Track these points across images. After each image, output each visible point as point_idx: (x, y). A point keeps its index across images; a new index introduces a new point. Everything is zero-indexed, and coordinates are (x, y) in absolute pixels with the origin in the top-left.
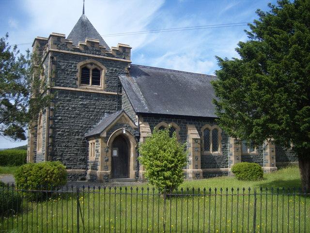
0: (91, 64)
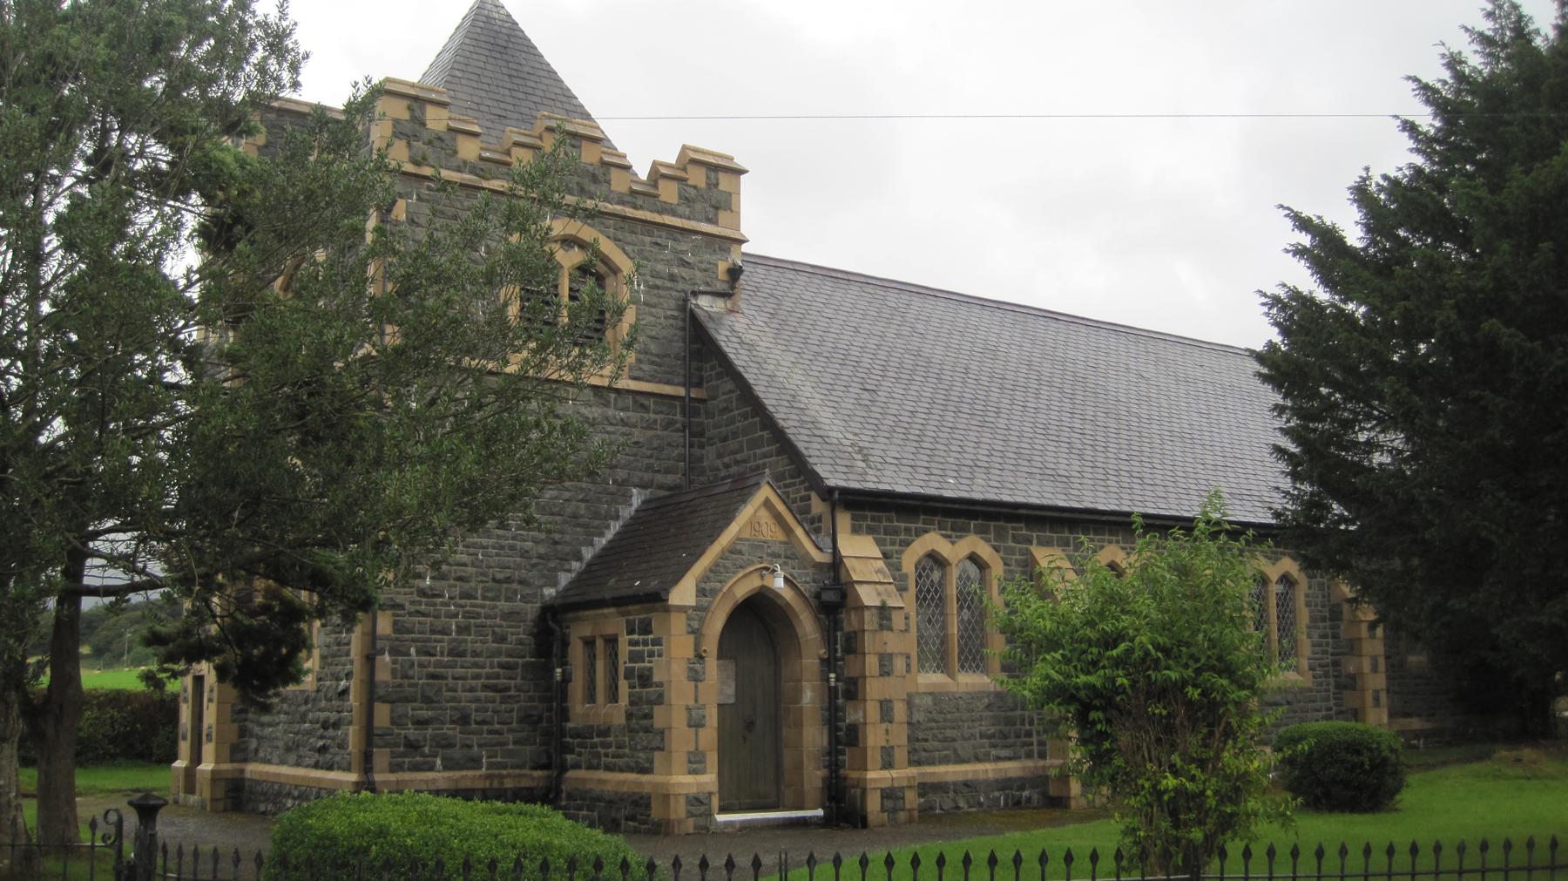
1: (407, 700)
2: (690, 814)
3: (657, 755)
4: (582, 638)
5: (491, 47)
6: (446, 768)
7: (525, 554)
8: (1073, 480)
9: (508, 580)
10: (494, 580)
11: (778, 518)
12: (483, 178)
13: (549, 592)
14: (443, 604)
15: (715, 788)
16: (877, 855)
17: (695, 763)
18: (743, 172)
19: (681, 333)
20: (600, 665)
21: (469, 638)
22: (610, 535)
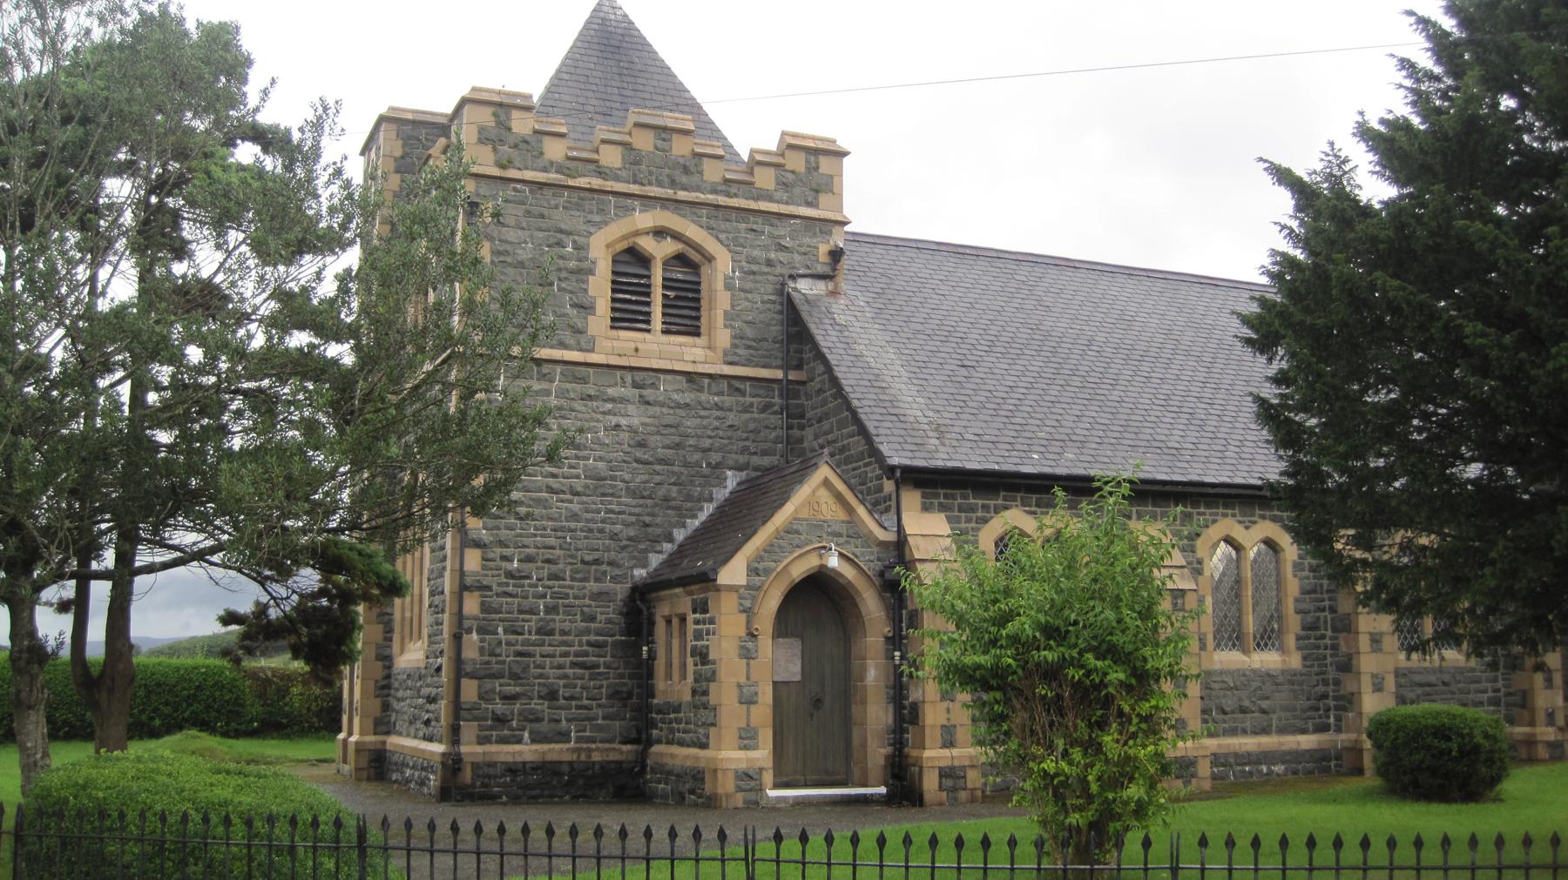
0: (660, 233)
1: (494, 676)
2: (739, 789)
3: (712, 730)
4: (663, 617)
5: (603, 48)
6: (533, 741)
7: (614, 537)
8: (1183, 452)
9: (597, 562)
10: (583, 562)
11: (839, 497)
12: (568, 176)
13: (640, 573)
14: (530, 585)
15: (769, 764)
16: (868, 834)
17: (747, 739)
18: (844, 154)
19: (778, 317)
20: (676, 643)
21: (557, 618)
22: (703, 516)
